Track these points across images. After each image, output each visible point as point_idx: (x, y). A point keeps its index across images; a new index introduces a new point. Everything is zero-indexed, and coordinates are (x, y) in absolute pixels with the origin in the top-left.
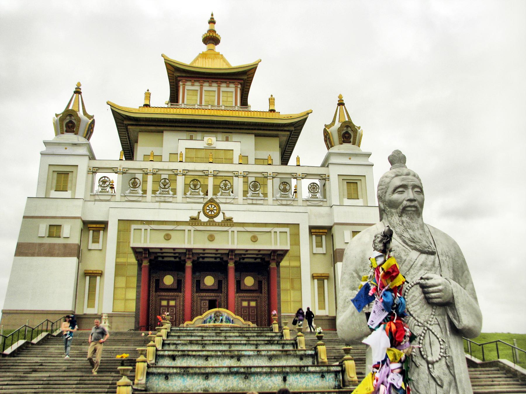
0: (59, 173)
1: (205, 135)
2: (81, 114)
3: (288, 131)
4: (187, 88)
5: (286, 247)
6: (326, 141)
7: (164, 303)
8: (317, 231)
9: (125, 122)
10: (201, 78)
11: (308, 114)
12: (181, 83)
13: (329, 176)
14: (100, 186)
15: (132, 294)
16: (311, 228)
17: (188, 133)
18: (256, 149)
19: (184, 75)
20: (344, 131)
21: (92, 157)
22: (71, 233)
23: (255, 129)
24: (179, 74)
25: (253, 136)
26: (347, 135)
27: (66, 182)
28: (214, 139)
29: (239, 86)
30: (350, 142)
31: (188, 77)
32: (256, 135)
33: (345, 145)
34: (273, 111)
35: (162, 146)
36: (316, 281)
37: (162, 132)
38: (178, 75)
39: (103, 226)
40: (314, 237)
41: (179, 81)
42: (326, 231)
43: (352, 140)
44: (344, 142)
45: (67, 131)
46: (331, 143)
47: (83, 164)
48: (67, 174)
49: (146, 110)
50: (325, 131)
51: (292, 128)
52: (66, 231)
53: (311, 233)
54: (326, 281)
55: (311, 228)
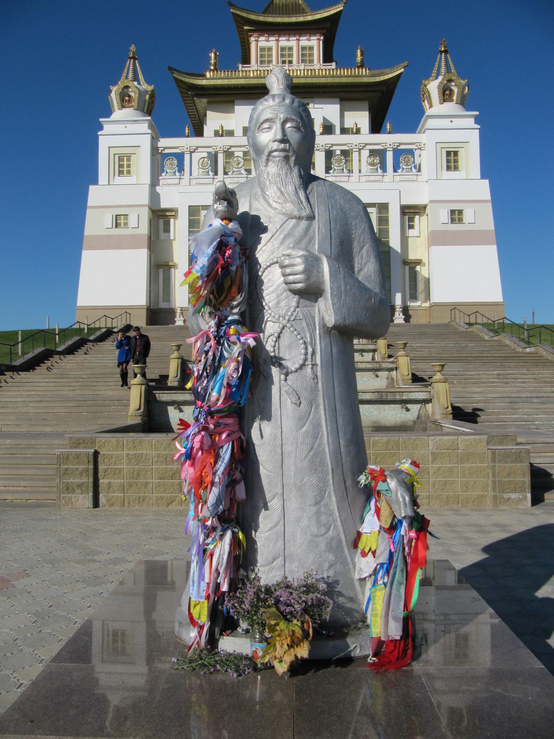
13: (424, 144)
33: (447, 104)
52: (132, 221)
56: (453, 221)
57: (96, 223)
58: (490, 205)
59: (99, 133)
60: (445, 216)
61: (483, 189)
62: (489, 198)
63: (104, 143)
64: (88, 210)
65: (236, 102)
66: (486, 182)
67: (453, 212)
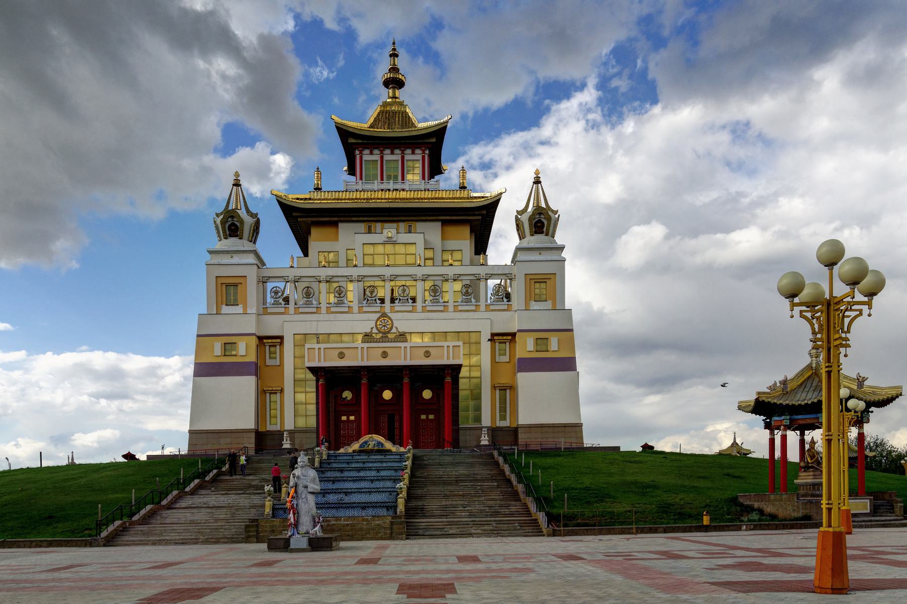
0: (228, 285)
1: (386, 225)
2: (242, 213)
4: (365, 158)
7: (344, 418)
11: (501, 194)
12: (357, 152)
14: (272, 297)
16: (493, 335)
21: (261, 263)
22: (245, 351)
24: (354, 141)
27: (236, 294)
30: (542, 233)
32: (445, 223)
34: (463, 188)
35: (337, 239)
38: (353, 143)
39: (278, 340)
42: (510, 338)
44: (536, 233)
45: (231, 236)
47: (252, 275)
49: (316, 195)
50: (517, 219)
55: (493, 335)
65: (340, 225)
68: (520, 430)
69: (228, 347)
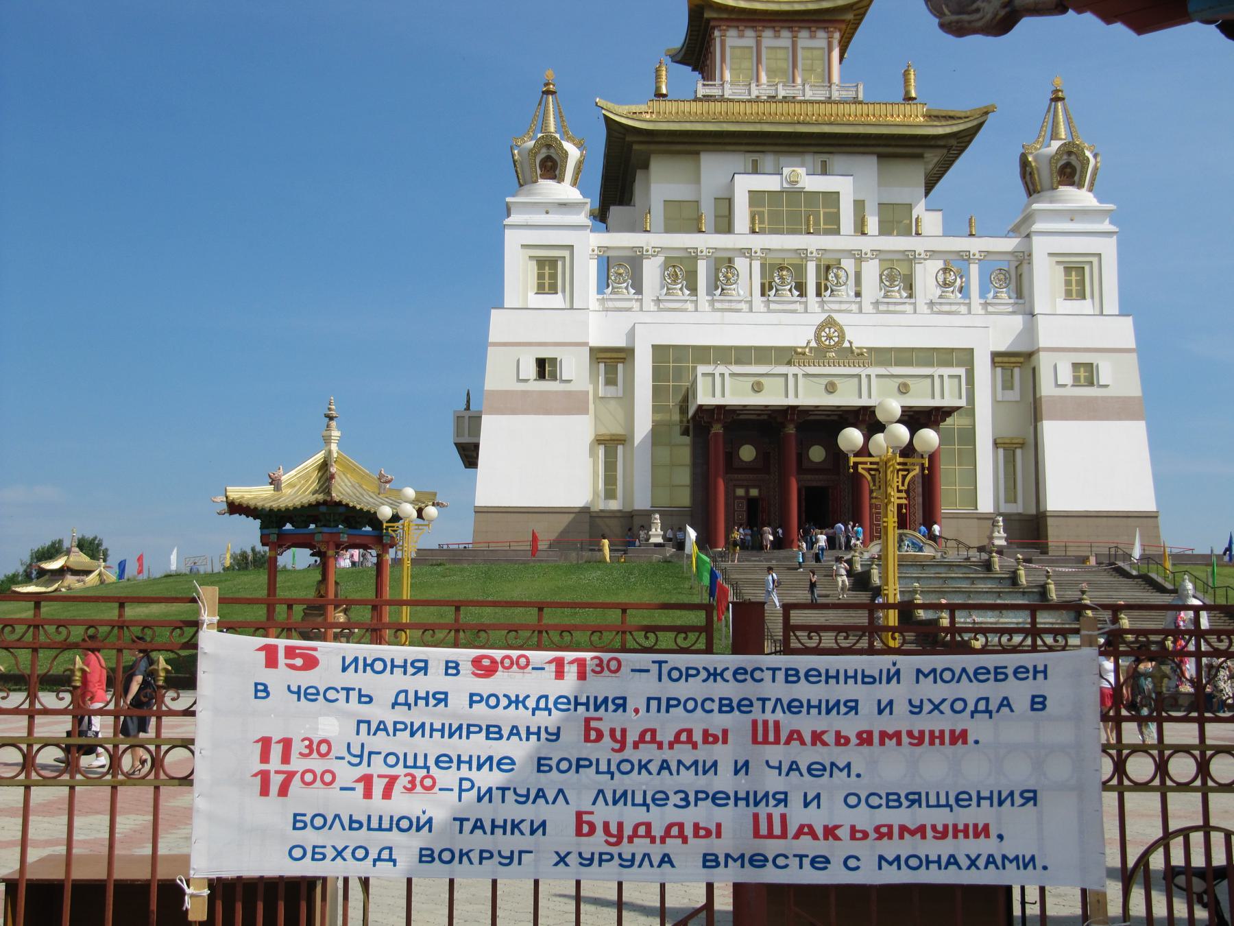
0: (541, 262)
1: (783, 159)
3: (944, 147)
5: (962, 403)
6: (1023, 176)
8: (1006, 359)
9: (628, 139)
10: (759, 20)
11: (987, 113)
12: (717, 33)
15: (684, 477)
16: (995, 355)
17: (748, 155)
18: (879, 185)
19: (725, 16)
20: (1062, 162)
23: (879, 146)
24: (715, 15)
25: (873, 160)
26: (1068, 170)
27: (554, 276)
28: (801, 171)
29: (837, 35)
31: (732, 20)
32: (881, 156)
36: (1001, 451)
37: (697, 153)
40: (999, 370)
41: (714, 28)
42: (1021, 360)
43: (1076, 178)
45: (543, 177)
46: (1034, 184)
48: (553, 262)
51: (953, 142)
53: (993, 363)
54: (1019, 452)
56: (1077, 382)
57: (504, 371)
58: (1134, 356)
59: (507, 221)
60: (1066, 376)
61: (1122, 332)
62: (1133, 345)
63: (513, 240)
64: (490, 349)
66: (1128, 322)
67: (1076, 366)
68: (1050, 521)
69: (544, 368)
